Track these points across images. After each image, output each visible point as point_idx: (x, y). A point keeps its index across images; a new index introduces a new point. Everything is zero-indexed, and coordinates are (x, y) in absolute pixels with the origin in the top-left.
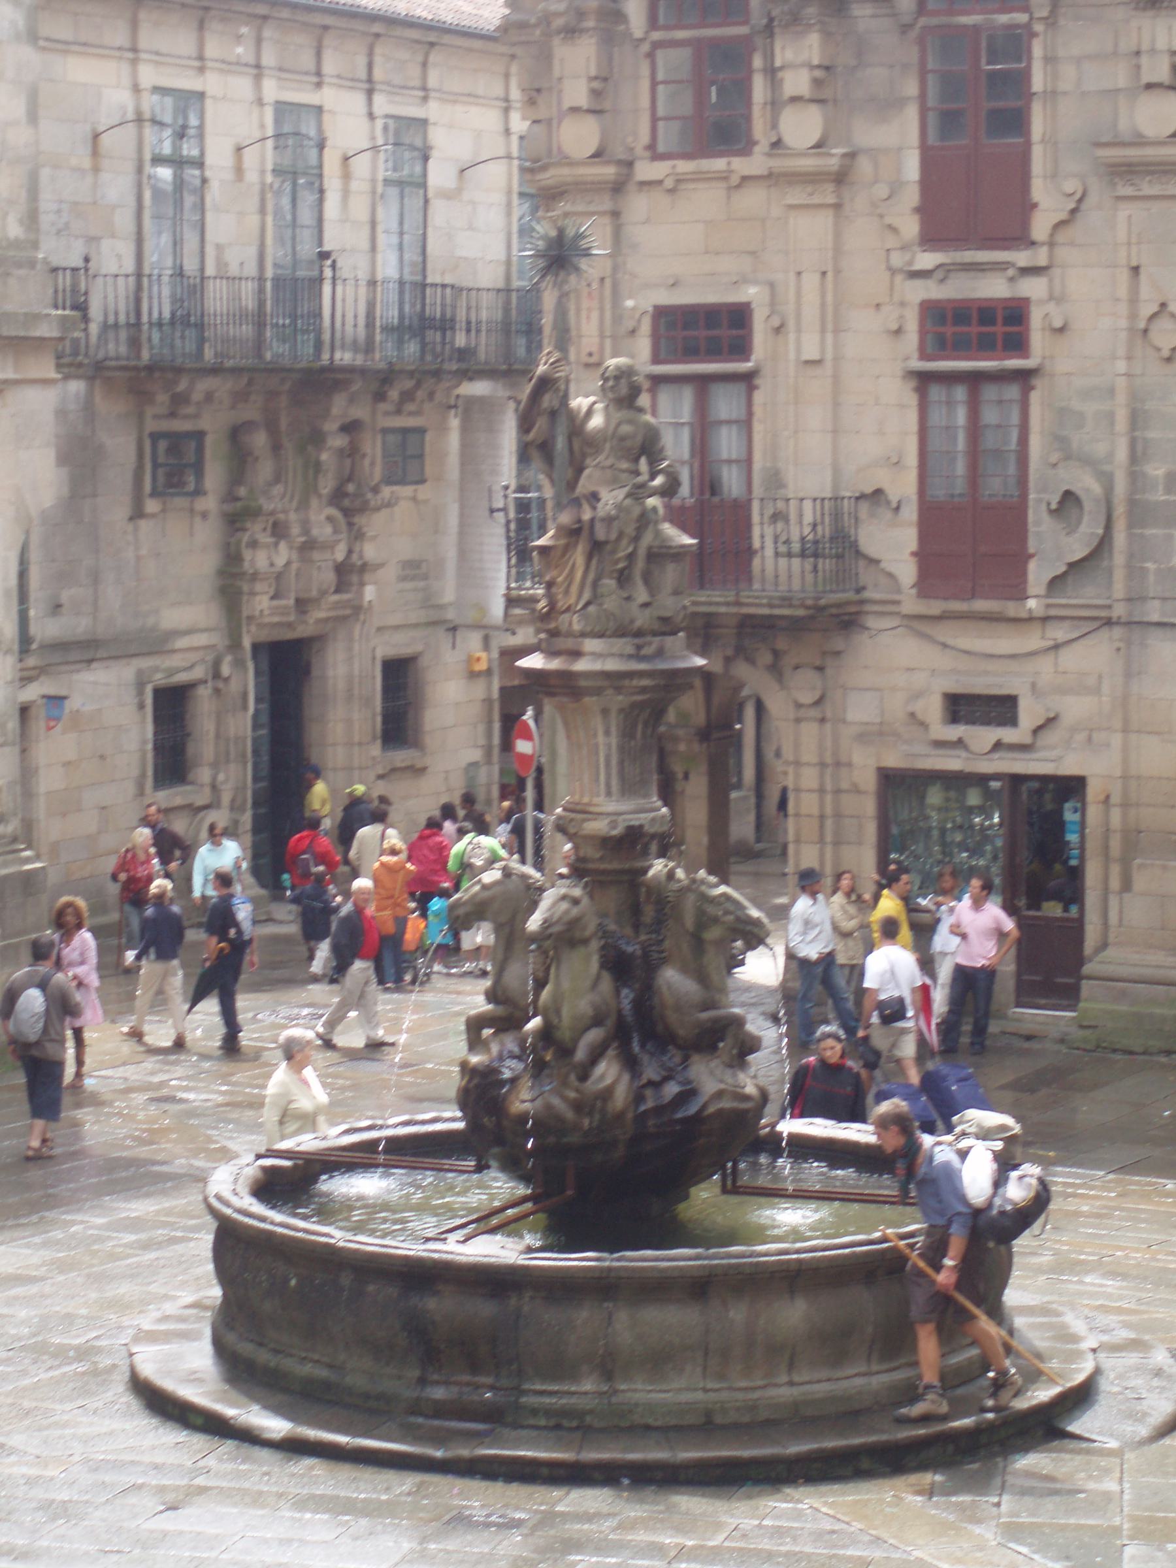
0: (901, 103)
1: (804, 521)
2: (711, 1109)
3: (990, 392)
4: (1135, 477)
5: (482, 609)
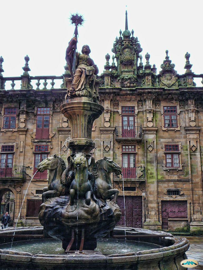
2: (115, 214)
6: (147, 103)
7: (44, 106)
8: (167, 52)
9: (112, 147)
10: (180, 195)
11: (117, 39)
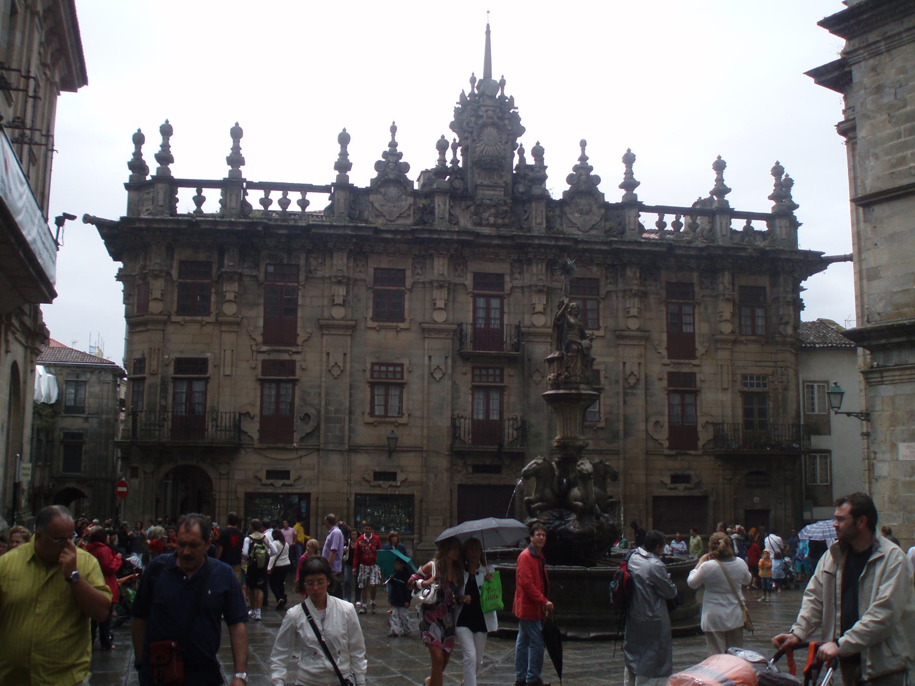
0: (258, 305)
1: (226, 421)
3: (283, 385)
4: (327, 411)
6: (534, 269)
7: (285, 262)
9: (450, 371)
11: (462, 95)
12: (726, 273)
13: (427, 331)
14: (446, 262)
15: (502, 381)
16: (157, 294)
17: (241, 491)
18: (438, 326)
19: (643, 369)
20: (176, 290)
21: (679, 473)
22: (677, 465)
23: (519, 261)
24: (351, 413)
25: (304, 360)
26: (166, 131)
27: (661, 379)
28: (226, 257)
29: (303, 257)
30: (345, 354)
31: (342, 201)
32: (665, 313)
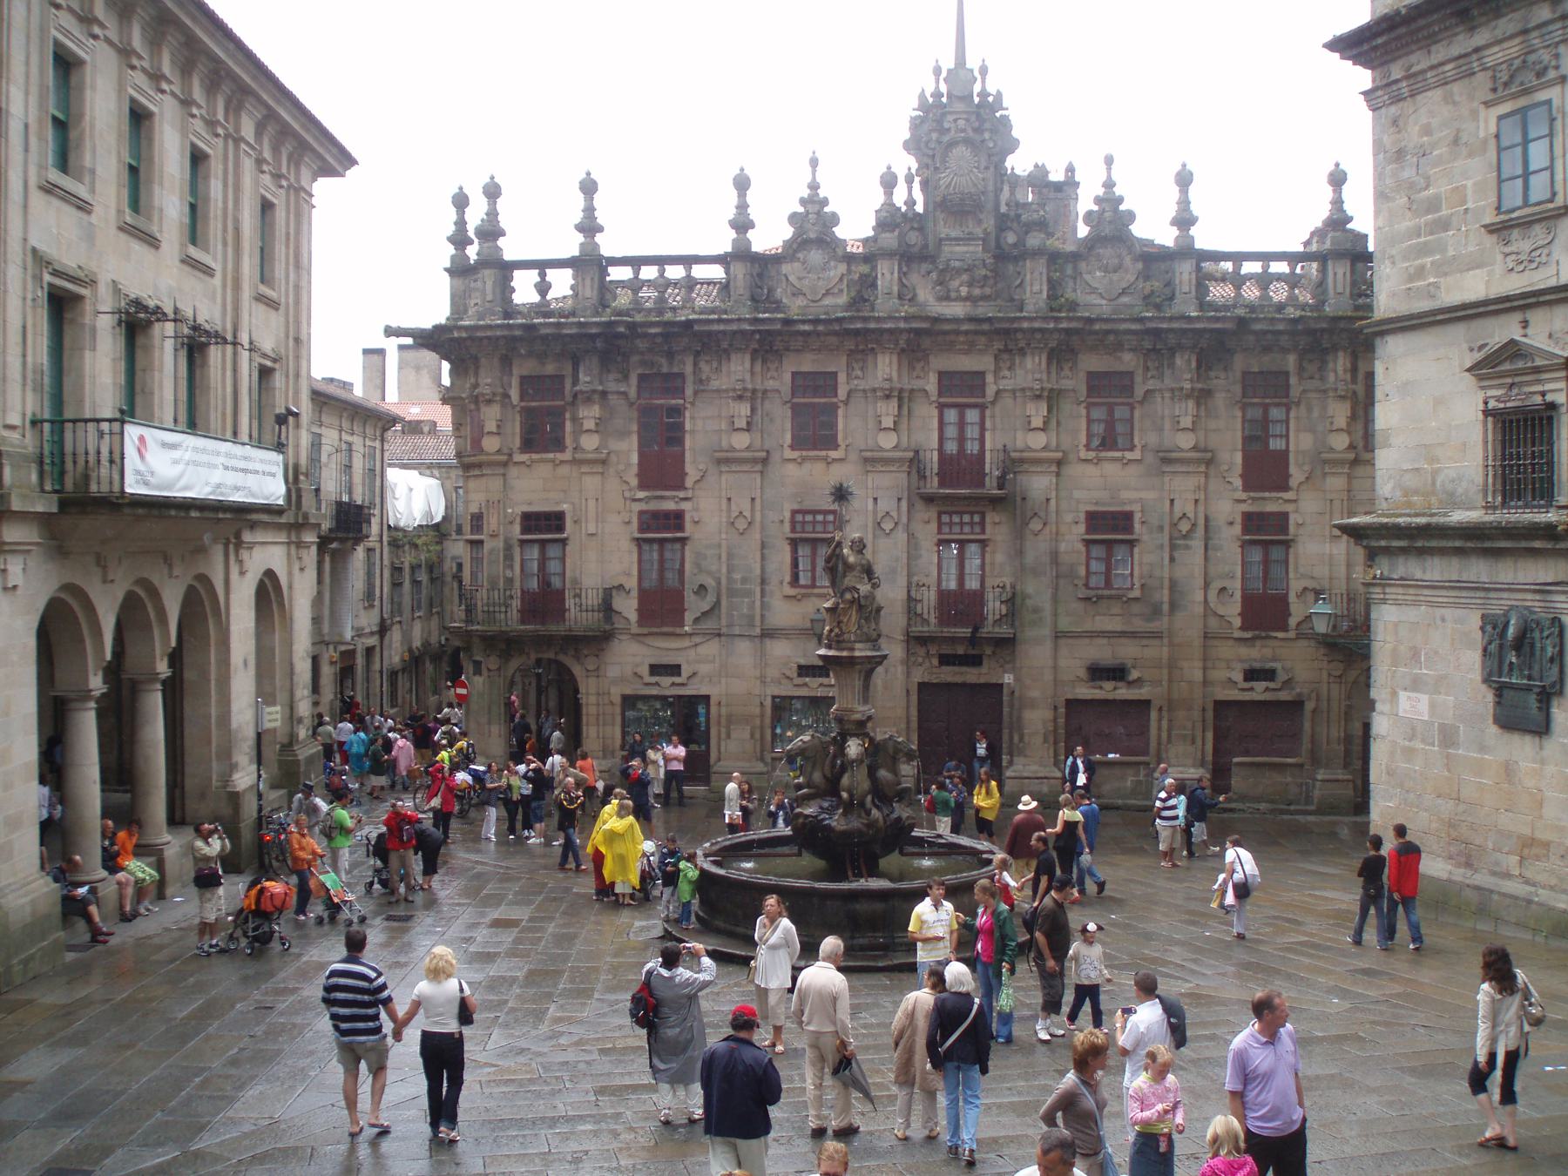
0: (630, 433)
1: (593, 599)
3: (668, 546)
4: (729, 579)
5: (341, 635)
7: (665, 370)
8: (1109, 161)
9: (904, 520)
10: (1130, 684)
11: (922, 96)
12: (1341, 354)
13: (872, 461)
14: (895, 358)
15: (983, 532)
16: (491, 426)
17: (616, 693)
18: (886, 454)
19: (1201, 508)
20: (518, 418)
21: (1257, 665)
22: (1256, 654)
23: (1007, 350)
24: (763, 582)
25: (696, 510)
26: (492, 192)
27: (1231, 523)
28: (581, 369)
29: (689, 361)
30: (753, 499)
31: (740, 276)
32: (1239, 420)
